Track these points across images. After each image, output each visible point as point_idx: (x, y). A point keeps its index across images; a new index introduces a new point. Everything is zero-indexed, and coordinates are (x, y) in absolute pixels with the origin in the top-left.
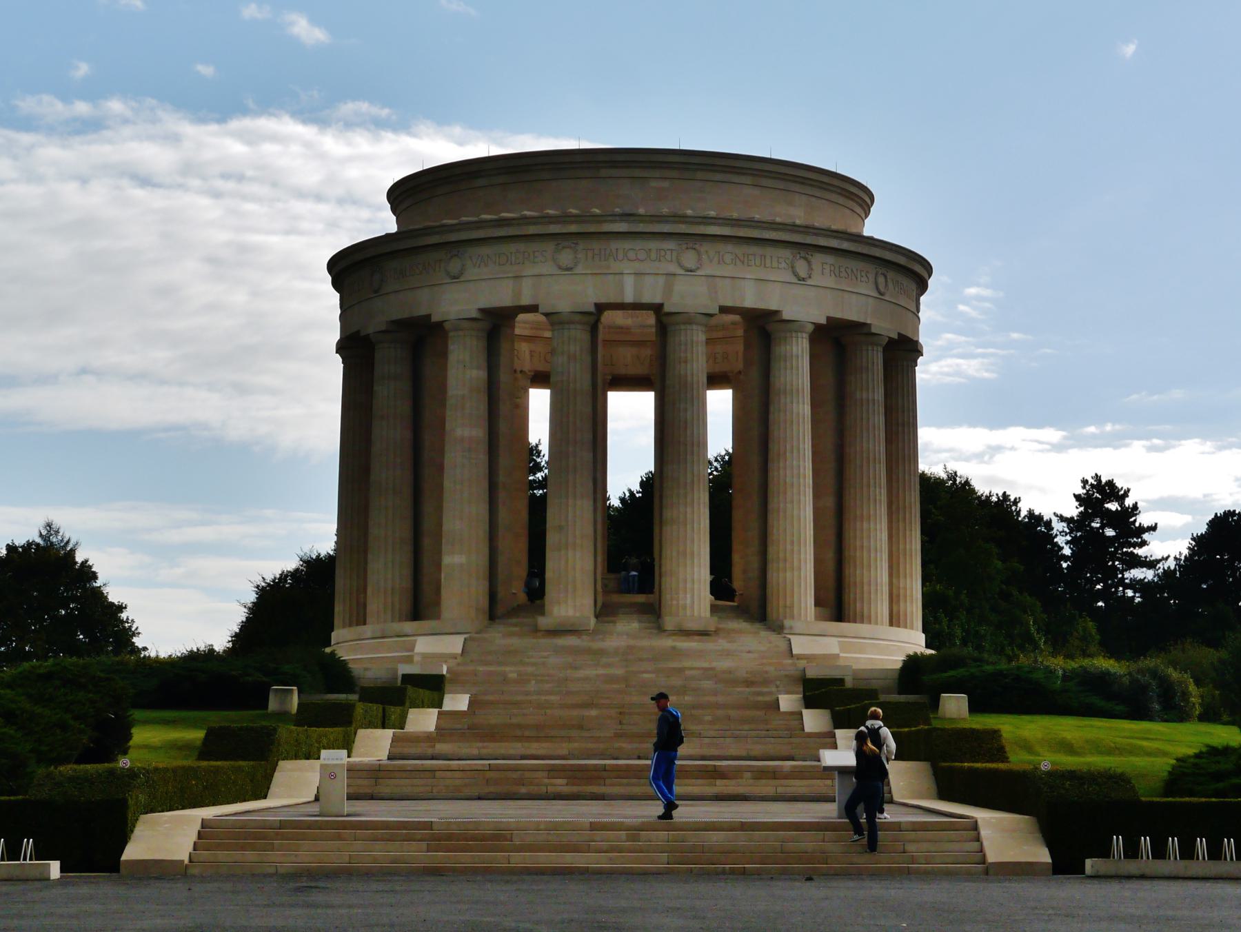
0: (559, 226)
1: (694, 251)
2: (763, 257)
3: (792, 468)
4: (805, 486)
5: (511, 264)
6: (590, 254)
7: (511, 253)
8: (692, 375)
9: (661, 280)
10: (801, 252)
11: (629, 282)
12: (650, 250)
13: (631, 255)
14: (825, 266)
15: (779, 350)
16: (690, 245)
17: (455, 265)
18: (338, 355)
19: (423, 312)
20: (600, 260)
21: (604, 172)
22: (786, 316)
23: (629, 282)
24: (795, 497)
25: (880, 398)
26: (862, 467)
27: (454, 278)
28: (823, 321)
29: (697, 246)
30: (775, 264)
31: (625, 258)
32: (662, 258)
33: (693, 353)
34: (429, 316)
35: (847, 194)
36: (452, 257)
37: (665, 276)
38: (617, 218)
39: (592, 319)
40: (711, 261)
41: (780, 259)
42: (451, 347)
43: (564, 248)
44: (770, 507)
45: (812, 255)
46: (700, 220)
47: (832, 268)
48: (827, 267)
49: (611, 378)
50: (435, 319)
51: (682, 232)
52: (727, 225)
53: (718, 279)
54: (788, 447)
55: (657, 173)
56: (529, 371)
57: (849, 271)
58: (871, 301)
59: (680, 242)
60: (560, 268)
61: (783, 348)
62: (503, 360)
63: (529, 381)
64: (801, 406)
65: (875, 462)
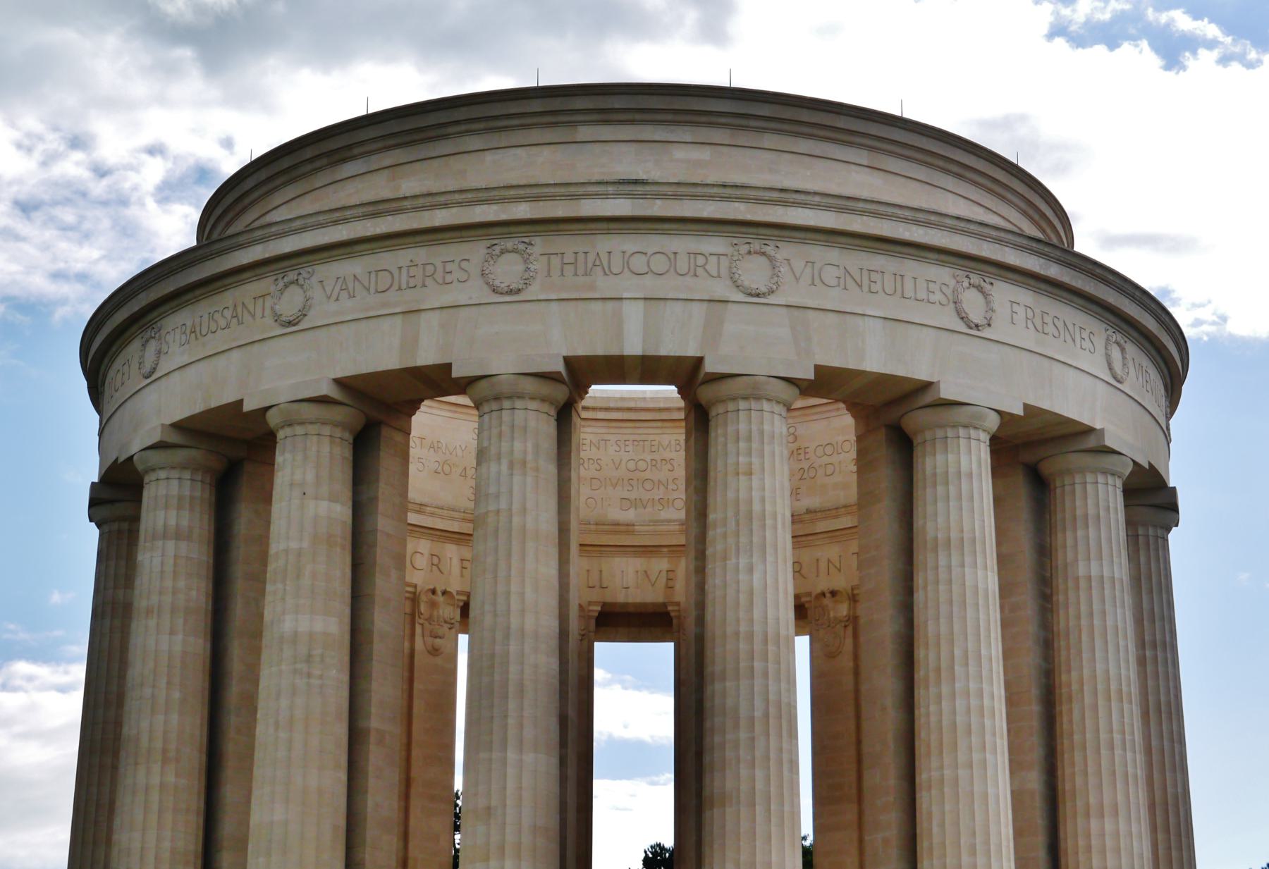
0: (495, 207)
1: (763, 259)
2: (898, 278)
3: (968, 695)
4: (994, 734)
5: (400, 289)
6: (556, 261)
7: (400, 268)
8: (763, 500)
9: (698, 310)
10: (971, 275)
11: (633, 314)
12: (675, 253)
13: (639, 263)
14: (1016, 307)
15: (930, 463)
16: (756, 245)
17: (290, 303)
18: (93, 524)
19: (228, 397)
20: (576, 274)
21: (585, 132)
22: (947, 392)
23: (633, 314)
24: (976, 757)
25: (1124, 578)
26: (1095, 708)
27: (290, 324)
28: (1018, 411)
29: (770, 250)
30: (922, 294)
31: (626, 269)
32: (700, 271)
33: (762, 456)
34: (241, 402)
35: (1036, 217)
36: (286, 286)
37: (705, 304)
38: (610, 189)
39: (561, 393)
40: (797, 279)
41: (931, 285)
42: (279, 459)
43: (502, 252)
44: (922, 777)
45: (992, 284)
46: (775, 195)
47: (1030, 314)
48: (1021, 311)
49: (599, 608)
50: (247, 407)
51: (740, 217)
52: (828, 208)
53: (811, 313)
54: (958, 652)
55: (685, 134)
56: (458, 593)
57: (1060, 325)
58: (1101, 385)
59: (735, 241)
60: (495, 291)
61: (940, 458)
62: (384, 490)
63: (459, 611)
64: (980, 573)
65: (1121, 700)
